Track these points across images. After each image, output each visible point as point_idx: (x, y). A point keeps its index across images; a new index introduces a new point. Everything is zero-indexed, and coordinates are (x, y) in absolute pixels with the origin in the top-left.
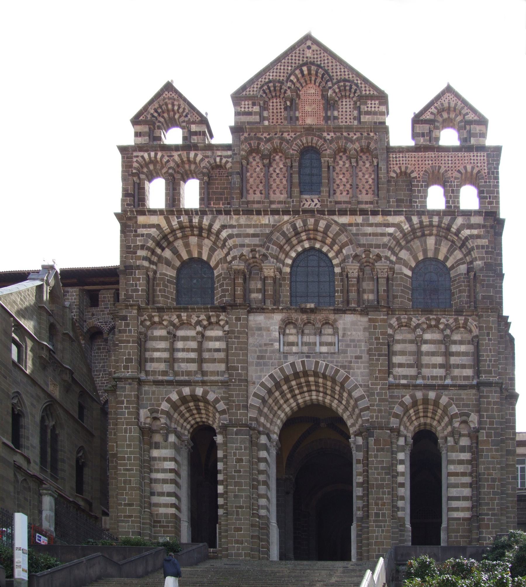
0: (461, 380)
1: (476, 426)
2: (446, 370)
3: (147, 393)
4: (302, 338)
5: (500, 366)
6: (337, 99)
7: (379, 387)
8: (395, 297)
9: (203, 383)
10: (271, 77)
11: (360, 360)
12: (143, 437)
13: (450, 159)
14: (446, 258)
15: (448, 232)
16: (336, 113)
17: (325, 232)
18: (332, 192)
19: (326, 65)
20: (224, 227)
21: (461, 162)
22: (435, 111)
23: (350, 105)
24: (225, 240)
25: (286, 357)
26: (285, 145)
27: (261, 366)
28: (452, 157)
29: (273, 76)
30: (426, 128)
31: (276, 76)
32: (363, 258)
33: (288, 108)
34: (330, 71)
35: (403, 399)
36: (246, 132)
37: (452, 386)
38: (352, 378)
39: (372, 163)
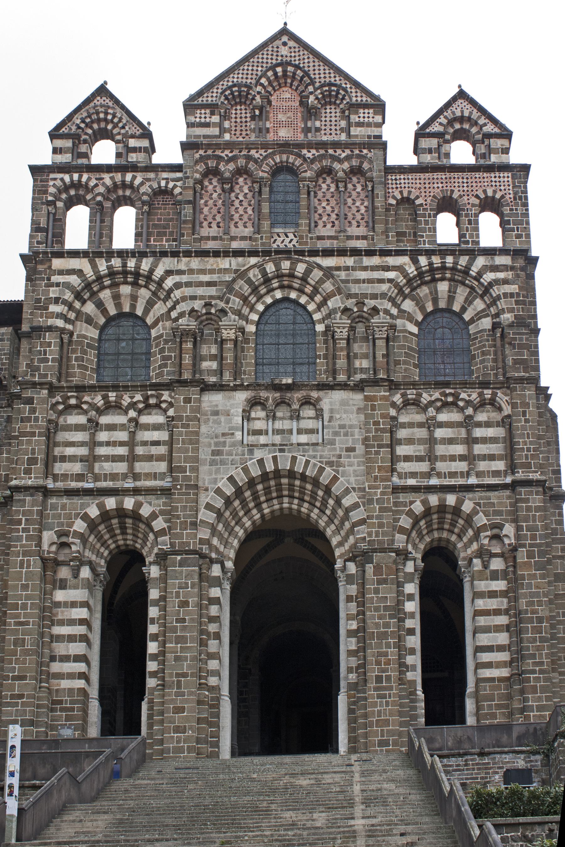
0: (489, 477)
1: (513, 541)
2: (469, 464)
3: (54, 507)
4: (273, 424)
5: (541, 456)
6: (319, 106)
7: (379, 491)
8: (397, 363)
9: (136, 491)
10: (235, 80)
11: (352, 454)
12: (44, 572)
13: (465, 181)
14: (464, 309)
15: (465, 276)
16: (318, 124)
17: (304, 279)
18: (313, 225)
19: (306, 65)
20: (169, 273)
21: (479, 184)
22: (445, 121)
23: (336, 113)
24: (170, 291)
25: (251, 452)
26: (252, 166)
27: (217, 464)
28: (467, 178)
29: (238, 78)
30: (433, 143)
31: (242, 78)
32: (354, 313)
33: (257, 118)
34: (311, 73)
35: (412, 507)
36: (202, 149)
37: (478, 486)
38: (341, 479)
39: (365, 187)
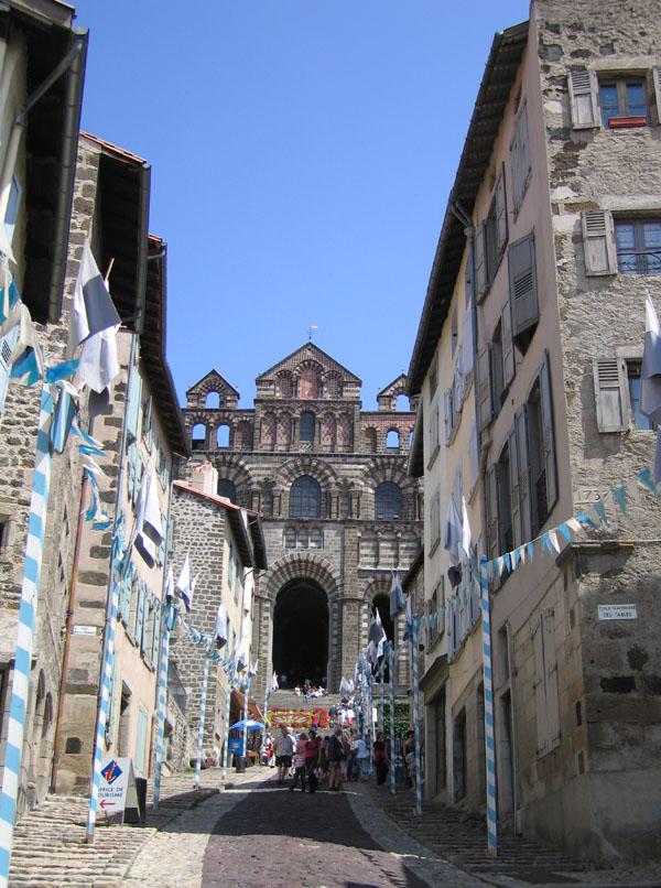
14: (399, 482)
17: (316, 468)
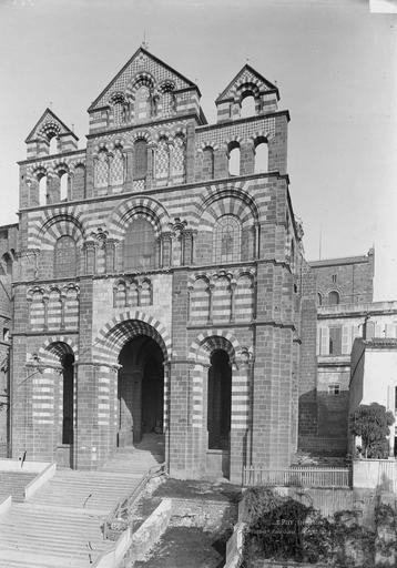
20: (81, 213)
